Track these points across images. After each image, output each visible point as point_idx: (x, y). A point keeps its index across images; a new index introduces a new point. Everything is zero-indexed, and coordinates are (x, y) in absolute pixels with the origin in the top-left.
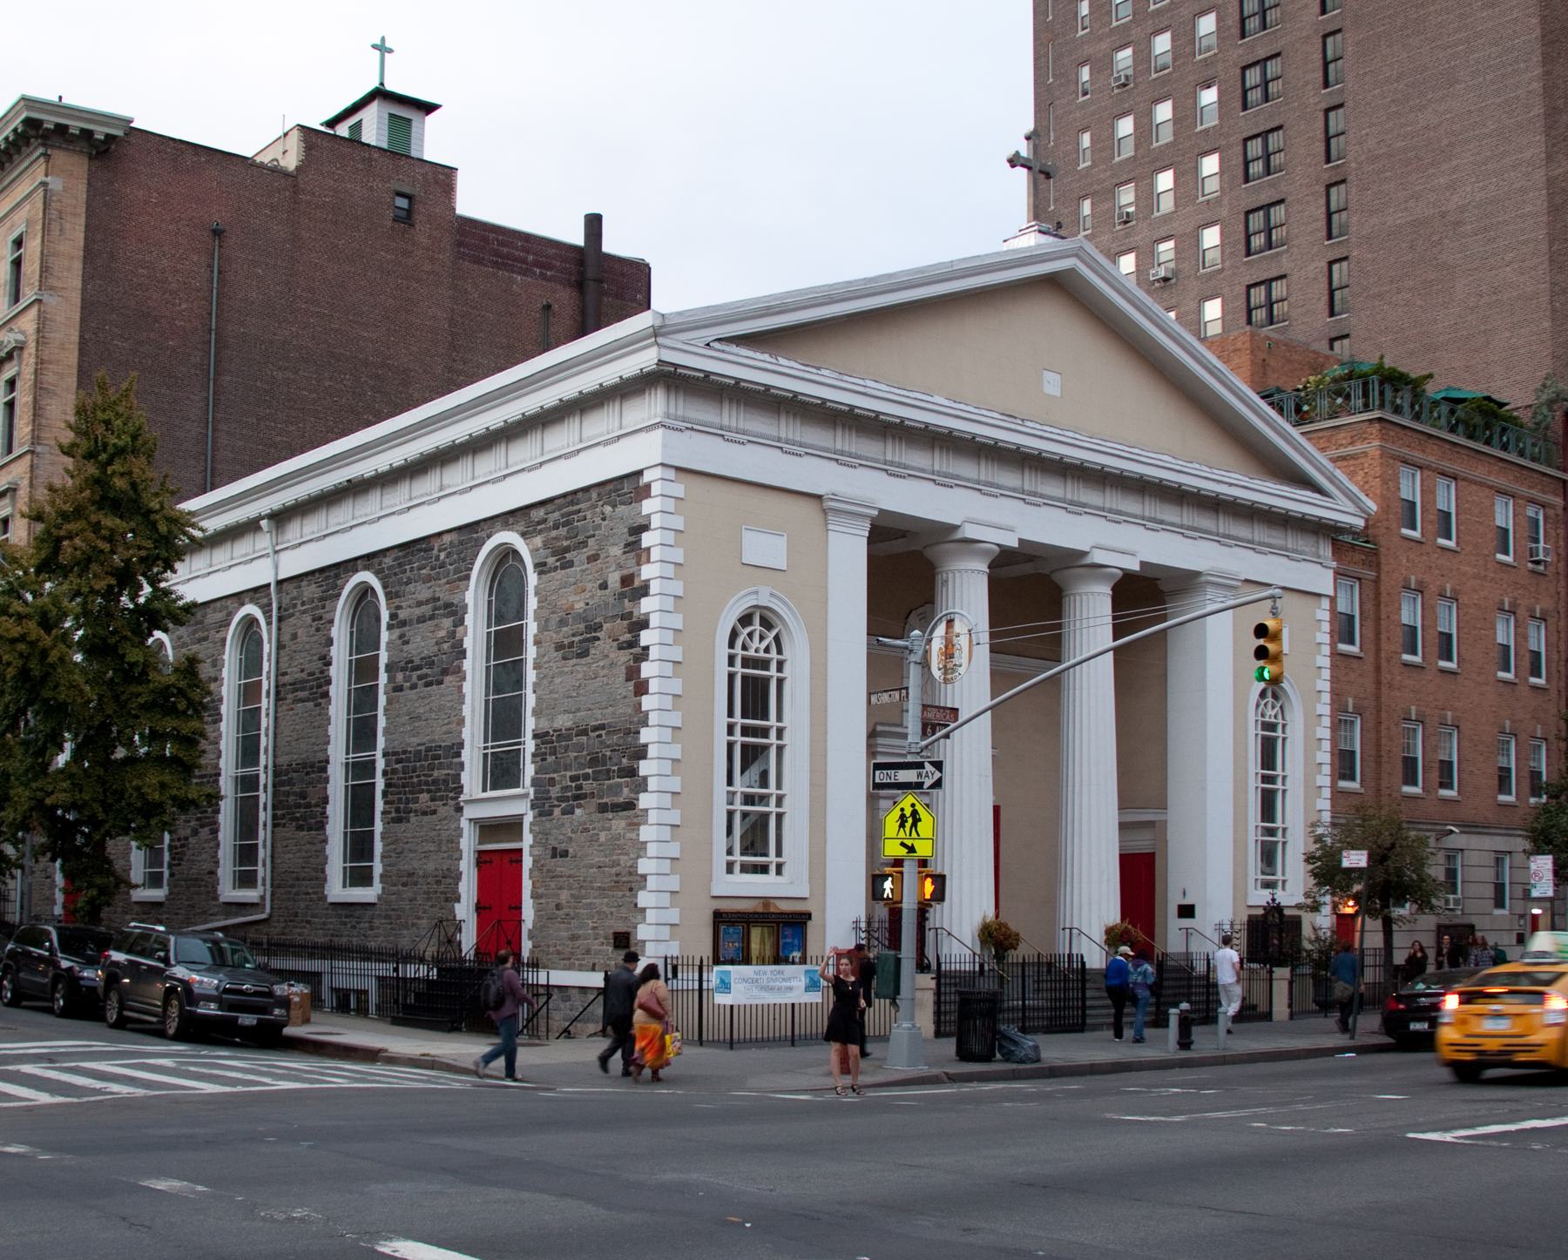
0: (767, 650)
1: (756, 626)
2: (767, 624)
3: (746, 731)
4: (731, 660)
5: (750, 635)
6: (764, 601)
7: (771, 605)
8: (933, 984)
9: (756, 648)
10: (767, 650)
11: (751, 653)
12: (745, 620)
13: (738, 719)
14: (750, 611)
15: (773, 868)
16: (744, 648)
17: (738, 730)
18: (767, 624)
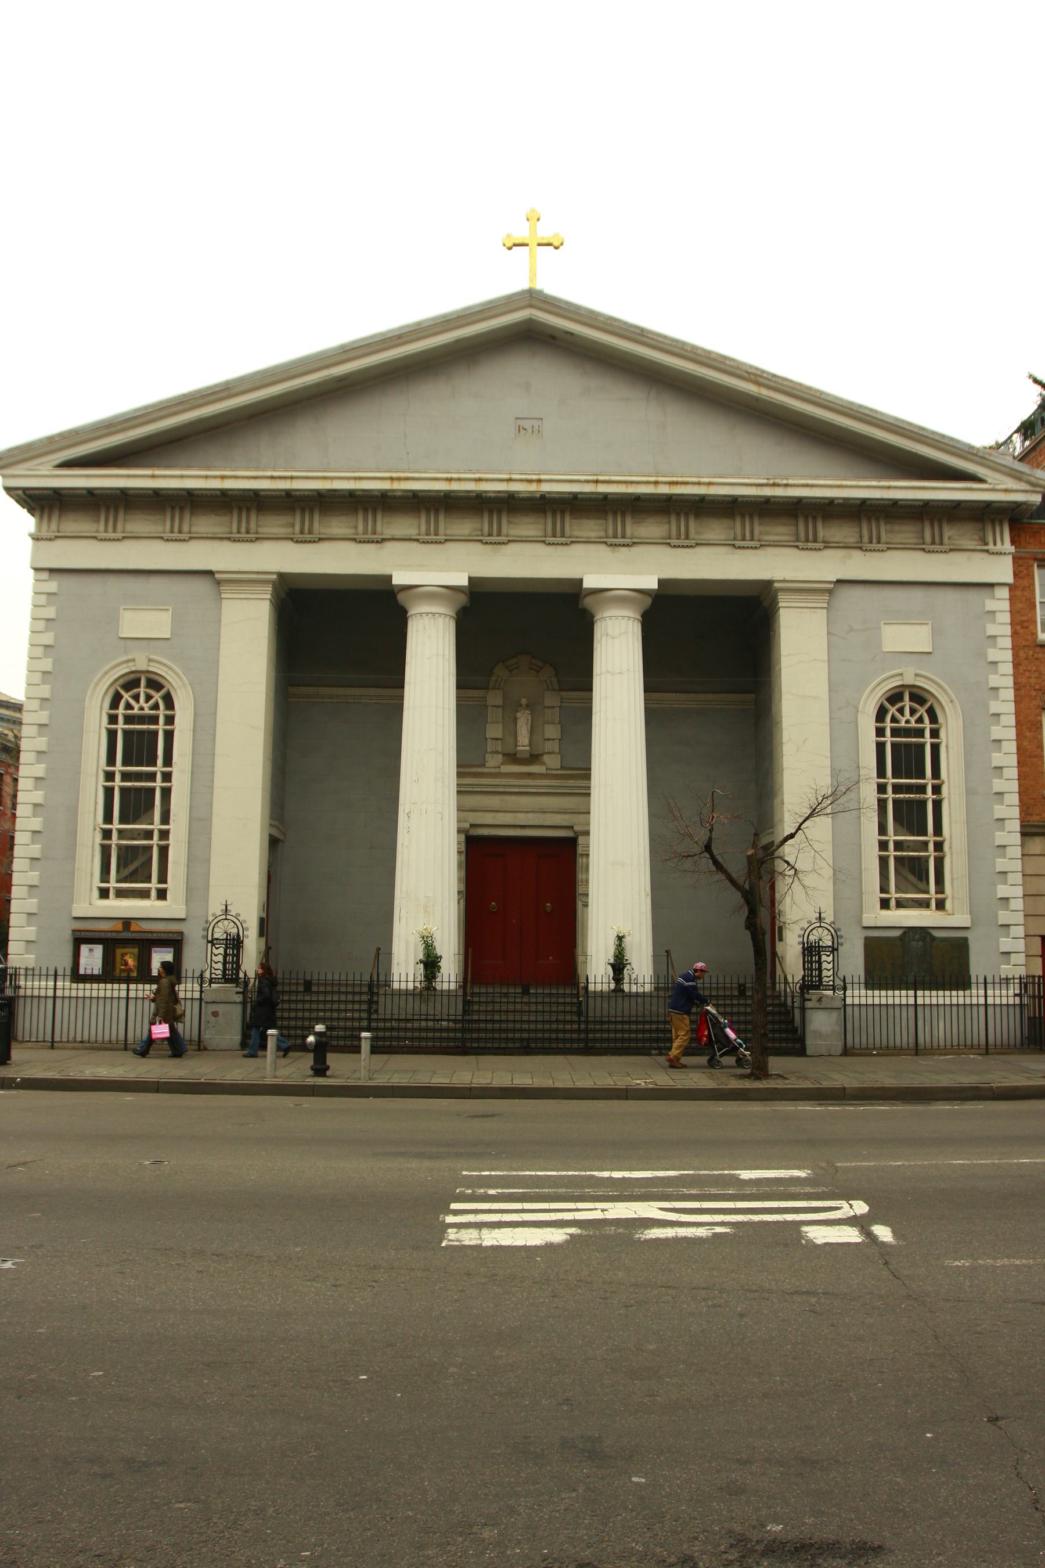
0: (920, 720)
1: (907, 703)
2: (155, 684)
3: (897, 789)
4: (880, 732)
5: (901, 711)
6: (909, 680)
7: (150, 669)
8: (239, 998)
9: (907, 720)
10: (156, 707)
11: (136, 711)
12: (895, 697)
13: (890, 780)
14: (132, 676)
15: (153, 893)
16: (894, 720)
17: (890, 789)
18: (914, 698)
